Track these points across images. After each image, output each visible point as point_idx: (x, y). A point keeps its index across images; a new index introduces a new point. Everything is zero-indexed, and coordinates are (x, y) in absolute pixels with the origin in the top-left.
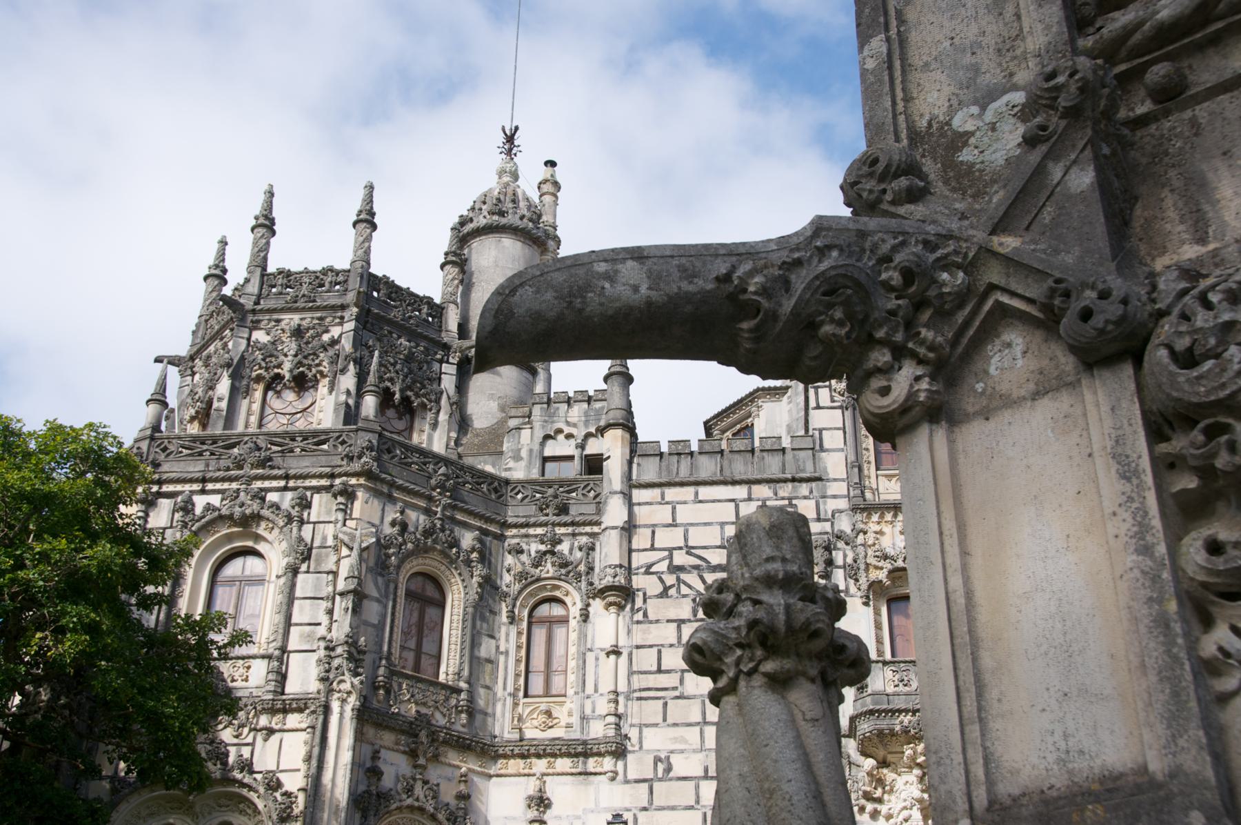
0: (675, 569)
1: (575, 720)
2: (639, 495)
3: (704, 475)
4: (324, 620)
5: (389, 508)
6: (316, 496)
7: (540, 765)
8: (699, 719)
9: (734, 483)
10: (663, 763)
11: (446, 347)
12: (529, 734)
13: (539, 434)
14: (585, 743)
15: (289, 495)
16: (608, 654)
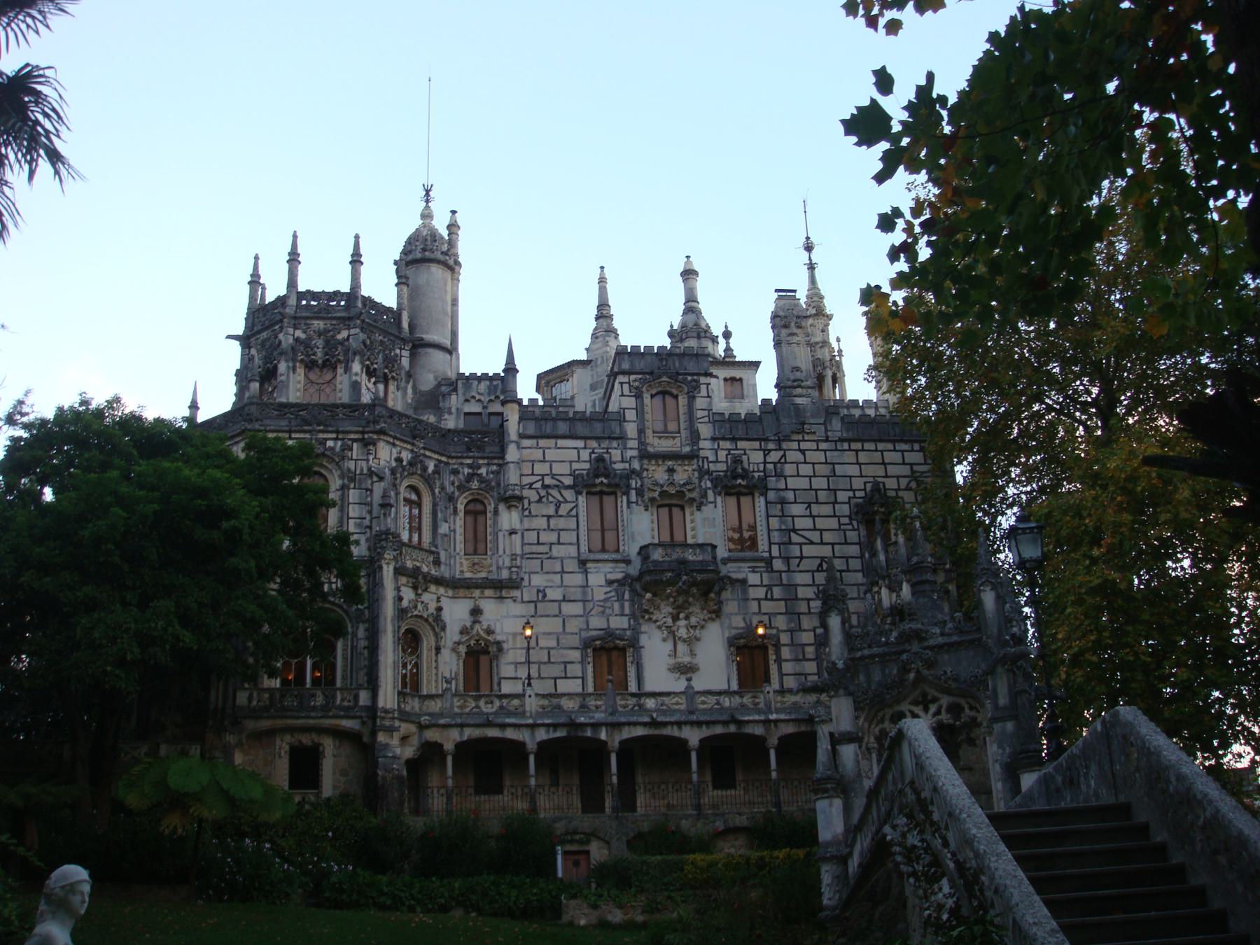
0: (545, 487)
1: (494, 568)
2: (526, 443)
3: (560, 432)
5: (394, 451)
6: (355, 445)
7: (477, 593)
8: (559, 569)
9: (576, 438)
10: (541, 592)
11: (403, 339)
12: (468, 575)
13: (461, 399)
14: (501, 581)
15: (339, 443)
16: (511, 534)
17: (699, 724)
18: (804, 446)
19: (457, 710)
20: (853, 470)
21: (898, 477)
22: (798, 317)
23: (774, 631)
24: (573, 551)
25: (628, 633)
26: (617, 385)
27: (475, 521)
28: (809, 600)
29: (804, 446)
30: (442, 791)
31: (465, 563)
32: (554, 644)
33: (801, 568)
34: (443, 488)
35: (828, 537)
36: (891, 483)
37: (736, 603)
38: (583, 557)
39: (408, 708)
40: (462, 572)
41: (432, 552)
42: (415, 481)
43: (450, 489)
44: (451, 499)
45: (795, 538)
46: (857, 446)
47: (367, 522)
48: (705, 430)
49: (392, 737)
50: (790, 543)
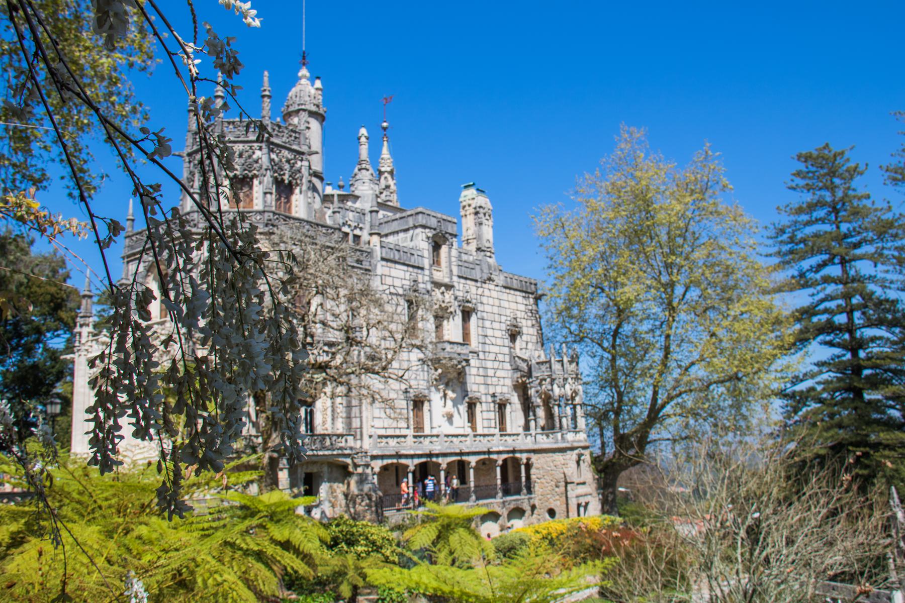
0: (391, 293)
35: (499, 342)
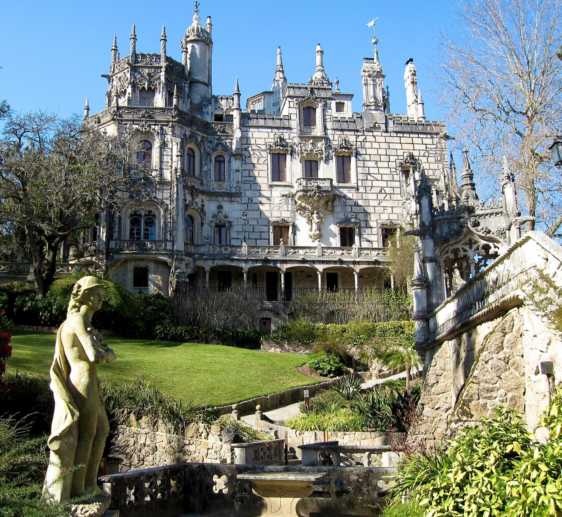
1: (228, 187)
4: (170, 161)
7: (220, 199)
14: (232, 193)
15: (157, 126)
17: (323, 262)
18: (375, 134)
19: (211, 252)
20: (398, 146)
21: (419, 150)
22: (375, 71)
23: (358, 221)
24: (265, 180)
25: (290, 219)
26: (287, 103)
27: (220, 166)
28: (375, 207)
29: (375, 134)
30: (204, 289)
31: (215, 185)
32: (255, 223)
33: (372, 192)
34: (205, 149)
35: (385, 177)
36: (416, 153)
37: (341, 207)
38: (270, 183)
39: (189, 251)
40: (213, 189)
41: (200, 179)
42: (192, 145)
43: (208, 150)
44: (208, 154)
45: (369, 177)
46: (401, 135)
47: (170, 164)
48: (329, 125)
49: (182, 263)
50: (367, 180)
